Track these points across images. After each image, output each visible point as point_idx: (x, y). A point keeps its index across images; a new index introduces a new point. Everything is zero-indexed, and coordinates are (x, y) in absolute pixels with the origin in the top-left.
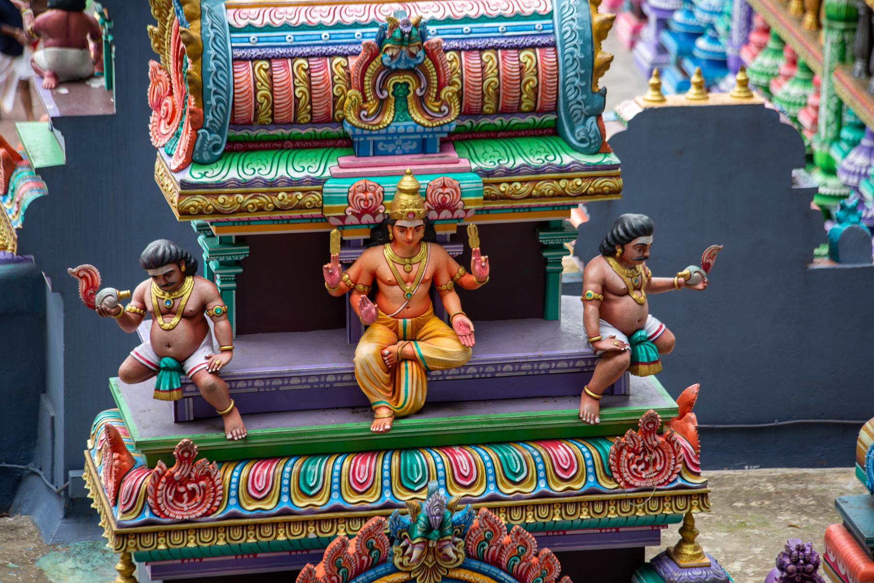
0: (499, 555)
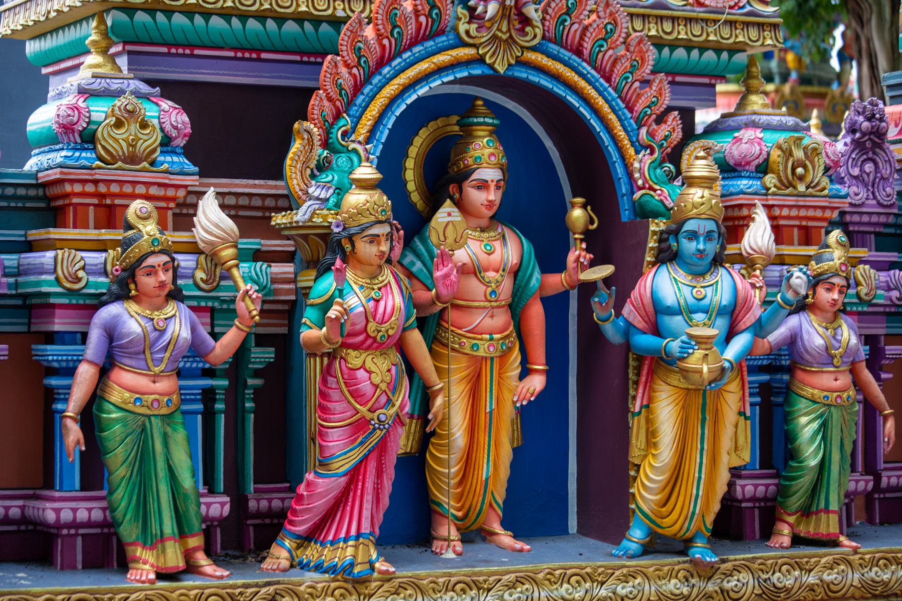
0: (582, 38)
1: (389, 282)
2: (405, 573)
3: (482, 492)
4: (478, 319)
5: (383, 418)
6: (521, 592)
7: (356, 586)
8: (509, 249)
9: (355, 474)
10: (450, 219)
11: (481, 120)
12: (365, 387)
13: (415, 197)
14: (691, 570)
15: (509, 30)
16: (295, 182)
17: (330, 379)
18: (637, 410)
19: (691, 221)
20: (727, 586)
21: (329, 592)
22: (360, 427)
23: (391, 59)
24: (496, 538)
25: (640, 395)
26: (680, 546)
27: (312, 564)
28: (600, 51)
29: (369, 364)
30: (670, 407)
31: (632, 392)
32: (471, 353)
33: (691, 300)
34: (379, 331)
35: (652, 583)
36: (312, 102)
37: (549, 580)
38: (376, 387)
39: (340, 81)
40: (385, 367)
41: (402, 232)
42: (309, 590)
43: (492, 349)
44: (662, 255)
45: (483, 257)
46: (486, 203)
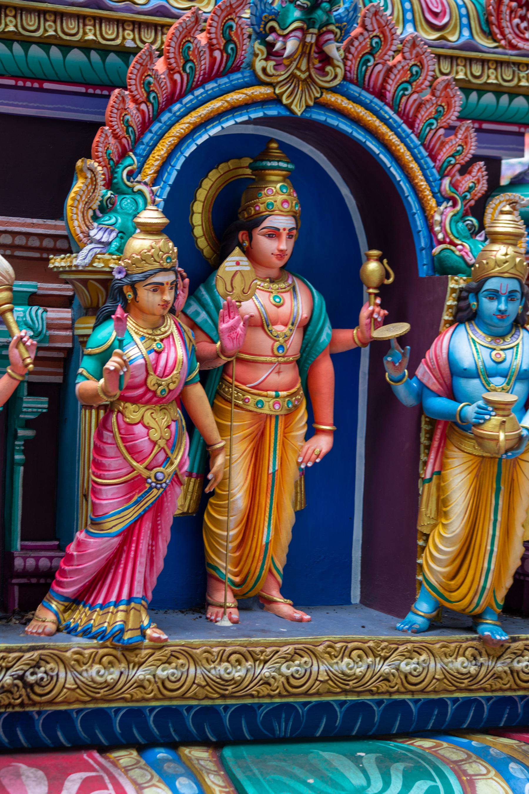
0: (385, 81)
1: (172, 334)
2: (178, 641)
3: (262, 557)
4: (263, 375)
5: (160, 476)
6: (299, 665)
7: (126, 653)
8: (299, 302)
9: (129, 535)
10: (238, 268)
11: (275, 164)
12: (143, 443)
13: (202, 243)
14: (480, 647)
15: (308, 69)
16: (76, 223)
17: (106, 433)
18: (428, 476)
19: (493, 280)
20: (518, 666)
21: (97, 659)
22: (135, 485)
23: (182, 95)
24: (274, 606)
25: (431, 461)
26: (469, 622)
27: (79, 629)
28: (404, 95)
29: (148, 419)
30: (463, 475)
31: (423, 457)
32: (255, 410)
33: (489, 363)
34: (160, 385)
35: (438, 660)
36: (96, 139)
37: (329, 653)
38: (155, 443)
39: (128, 117)
40: (164, 423)
41: (187, 280)
42: (75, 656)
43: (277, 407)
44: (460, 314)
45: (272, 310)
46: (276, 252)
